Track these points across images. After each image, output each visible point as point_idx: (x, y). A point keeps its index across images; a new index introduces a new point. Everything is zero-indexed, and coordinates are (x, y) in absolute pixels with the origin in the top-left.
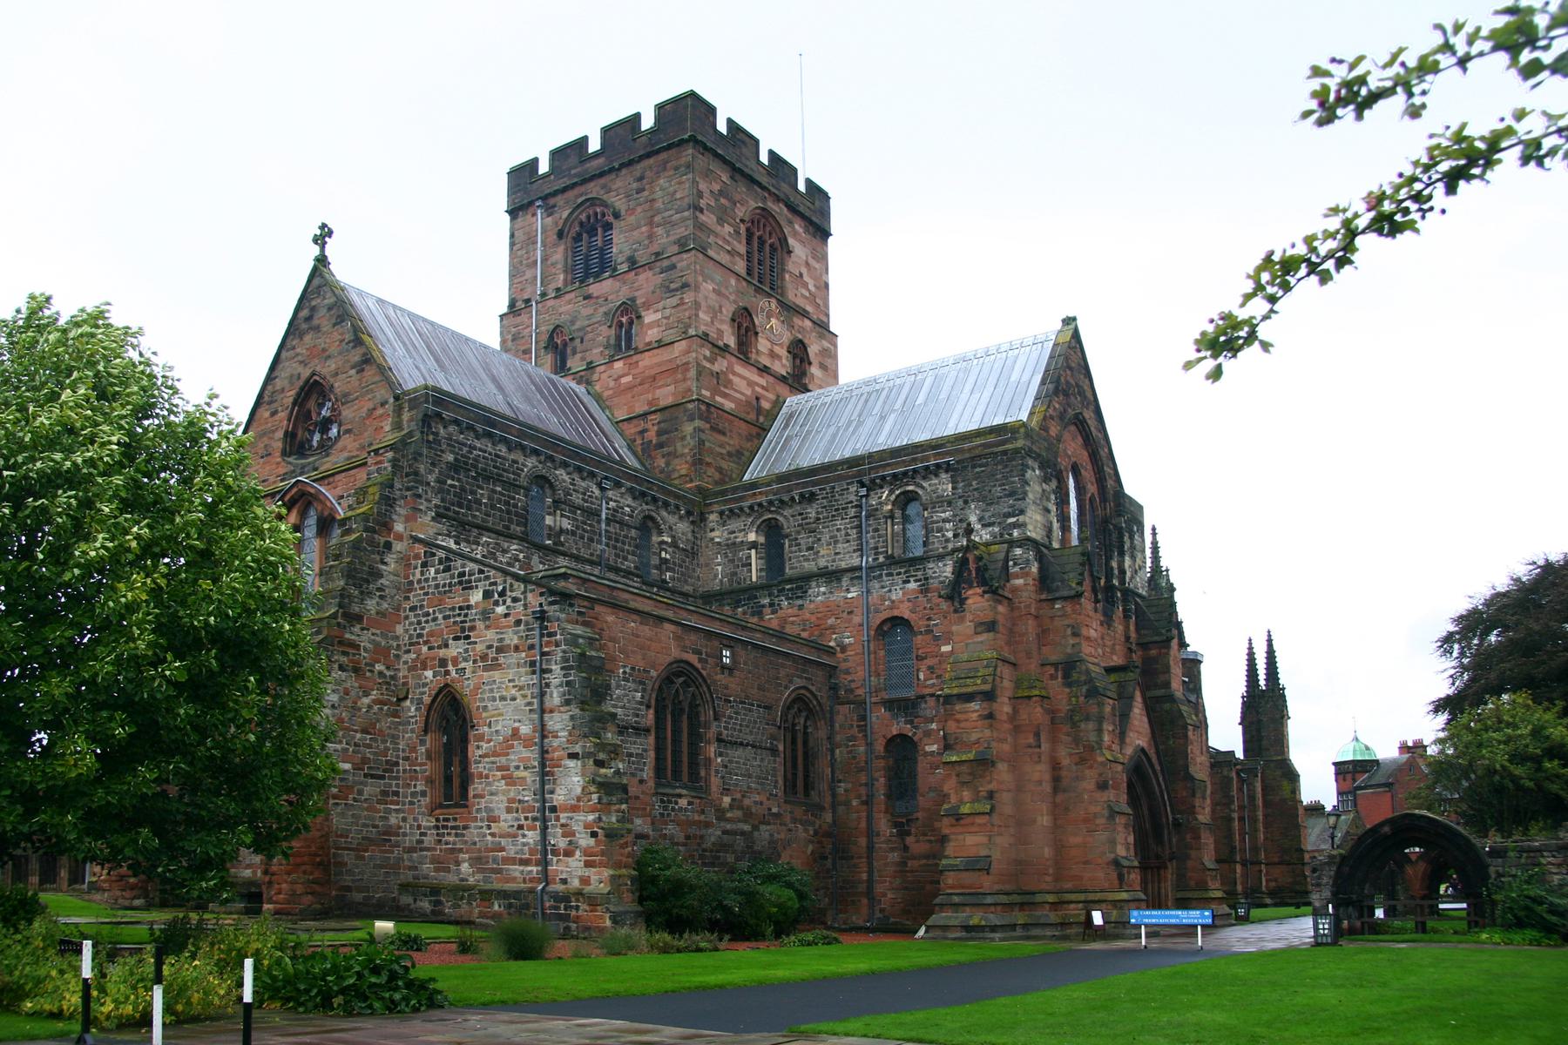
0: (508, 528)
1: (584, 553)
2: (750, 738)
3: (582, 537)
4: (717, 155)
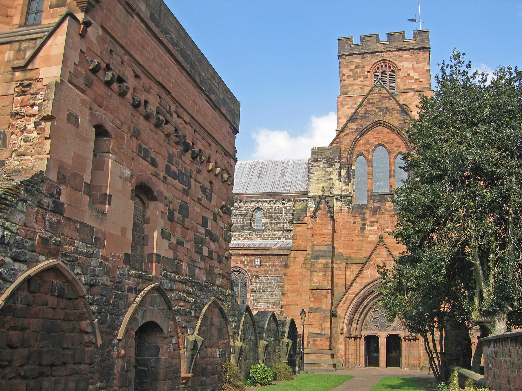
0: (244, 228)
1: (275, 228)
2: (269, 289)
3: (274, 223)
4: (346, 55)
